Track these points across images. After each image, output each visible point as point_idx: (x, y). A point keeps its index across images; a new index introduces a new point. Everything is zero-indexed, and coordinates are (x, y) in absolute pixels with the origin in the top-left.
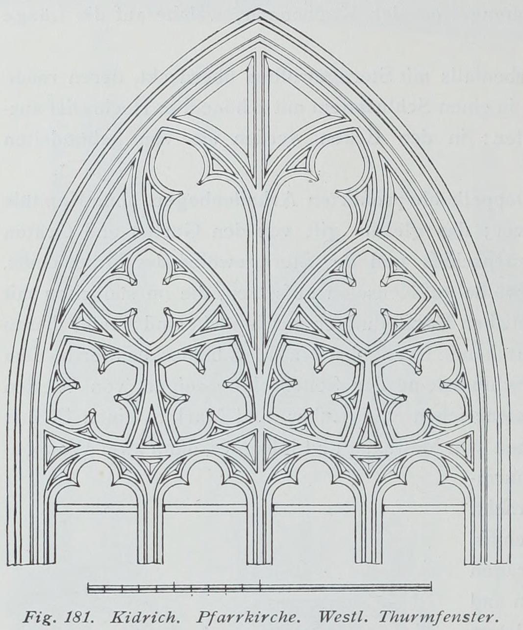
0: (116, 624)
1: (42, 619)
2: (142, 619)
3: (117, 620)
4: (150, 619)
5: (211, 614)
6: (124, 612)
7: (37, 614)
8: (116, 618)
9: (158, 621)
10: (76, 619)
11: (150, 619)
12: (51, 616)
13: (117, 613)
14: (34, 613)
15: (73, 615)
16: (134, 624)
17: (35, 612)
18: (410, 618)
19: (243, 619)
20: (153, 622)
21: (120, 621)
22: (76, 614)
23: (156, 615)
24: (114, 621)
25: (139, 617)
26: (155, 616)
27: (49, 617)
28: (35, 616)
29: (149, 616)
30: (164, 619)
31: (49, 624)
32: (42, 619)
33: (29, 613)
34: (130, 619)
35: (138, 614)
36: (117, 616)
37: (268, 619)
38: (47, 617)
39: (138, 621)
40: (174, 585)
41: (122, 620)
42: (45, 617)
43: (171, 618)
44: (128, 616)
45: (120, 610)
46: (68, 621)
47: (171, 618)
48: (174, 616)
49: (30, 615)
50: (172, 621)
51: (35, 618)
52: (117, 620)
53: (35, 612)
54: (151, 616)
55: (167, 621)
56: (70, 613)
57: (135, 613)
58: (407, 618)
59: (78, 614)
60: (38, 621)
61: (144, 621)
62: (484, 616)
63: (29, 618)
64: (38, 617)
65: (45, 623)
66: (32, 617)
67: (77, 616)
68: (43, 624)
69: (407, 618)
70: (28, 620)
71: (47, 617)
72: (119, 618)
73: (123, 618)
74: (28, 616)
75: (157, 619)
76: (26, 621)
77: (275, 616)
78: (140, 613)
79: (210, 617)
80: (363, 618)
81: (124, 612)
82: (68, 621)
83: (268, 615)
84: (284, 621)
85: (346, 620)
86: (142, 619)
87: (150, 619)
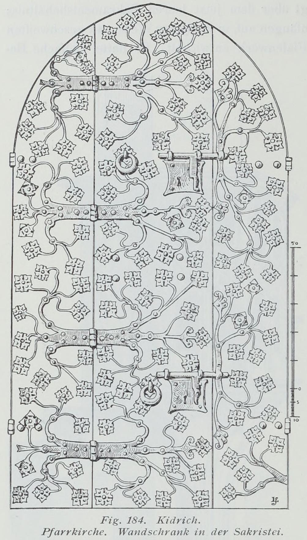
0: (160, 525)
1: (112, 521)
2: (176, 521)
3: (160, 522)
6: (165, 517)
7: (110, 518)
9: (186, 522)
10: (134, 521)
12: (118, 520)
13: (160, 517)
15: (132, 519)
17: (108, 517)
20: (183, 523)
21: (162, 523)
22: (134, 519)
23: (185, 519)
24: (158, 523)
25: (174, 520)
26: (184, 520)
28: (108, 519)
31: (117, 524)
32: (112, 521)
33: (104, 517)
34: (169, 522)
35: (174, 518)
36: (161, 519)
38: (116, 520)
41: (163, 522)
42: (114, 520)
45: (163, 516)
48: (196, 520)
49: (105, 519)
50: (195, 523)
51: (108, 521)
52: (160, 522)
53: (108, 517)
54: (182, 519)
56: (130, 518)
57: (172, 518)
59: (135, 518)
60: (110, 523)
61: (178, 523)
63: (104, 521)
64: (111, 520)
65: (115, 524)
66: (106, 520)
67: (134, 520)
68: (113, 524)
70: (104, 522)
71: (116, 520)
72: (161, 520)
73: (164, 521)
74: (103, 520)
75: (185, 521)
76: (102, 523)
78: (175, 517)
81: (165, 517)
82: (129, 523)
86: (176, 521)
87: (181, 522)
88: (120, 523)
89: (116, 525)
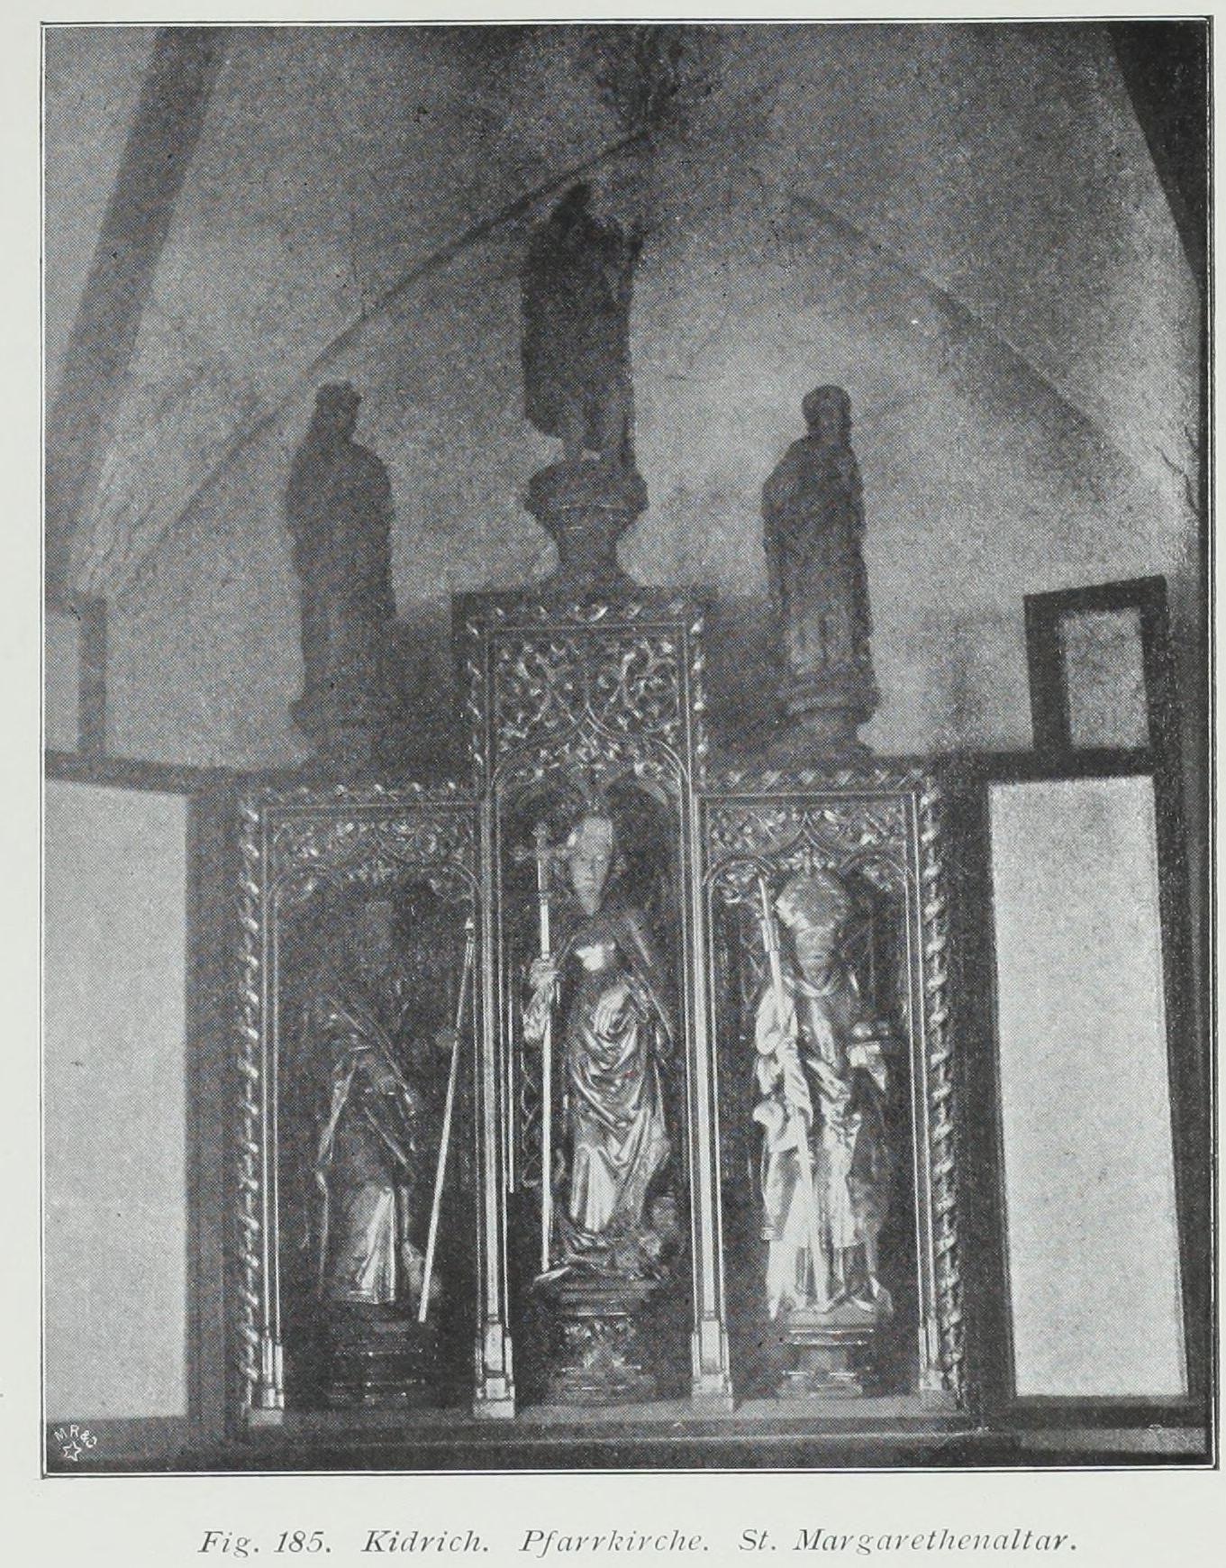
1: (232, 1546)
2: (419, 1543)
3: (373, 1546)
4: (435, 1544)
5: (546, 1536)
8: (372, 1543)
10: (296, 1546)
11: (433, 1545)
15: (290, 1539)
19: (603, 1545)
20: (439, 1549)
21: (379, 1549)
22: (295, 1538)
24: (367, 1549)
32: (232, 1546)
33: (210, 1534)
34: (398, 1544)
37: (650, 1545)
43: (473, 1542)
45: (380, 1528)
47: (473, 1542)
49: (212, 1538)
52: (373, 1546)
56: (285, 1536)
57: (406, 1534)
59: (300, 1537)
63: (210, 1544)
73: (385, 1543)
74: (208, 1541)
75: (446, 1546)
76: (204, 1549)
79: (545, 1540)
86: (419, 1543)
87: (433, 1545)
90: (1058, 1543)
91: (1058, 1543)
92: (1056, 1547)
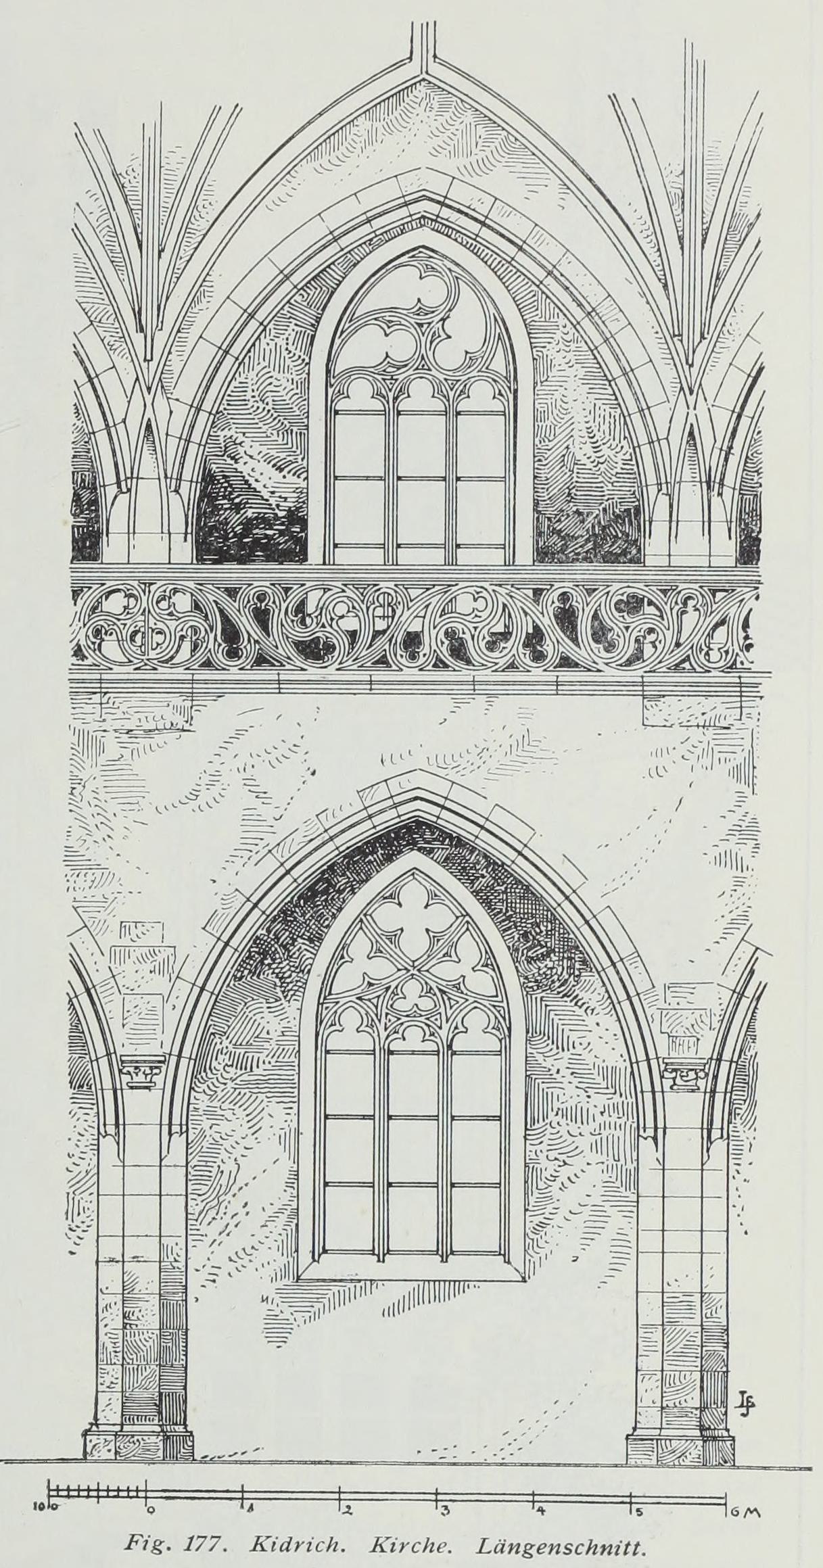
0: (258, 1554)
1: (150, 1546)
3: (259, 1548)
4: (305, 1546)
7: (146, 1538)
8: (258, 1545)
9: (315, 1549)
11: (304, 1547)
13: (259, 1537)
14: (140, 1537)
16: (282, 1553)
17: (142, 1536)
18: (507, 1549)
20: (308, 1550)
25: (289, 1543)
26: (310, 1543)
27: (161, 1543)
28: (141, 1541)
29: (303, 1543)
30: (323, 1547)
32: (150, 1546)
33: (133, 1536)
34: (277, 1547)
35: (288, 1540)
38: (157, 1543)
39: (287, 1550)
40: (243, 1492)
42: (155, 1542)
43: (332, 1546)
44: (274, 1543)
46: (188, 1549)
47: (332, 1546)
48: (337, 1543)
49: (135, 1539)
50: (334, 1550)
51: (141, 1544)
52: (259, 1548)
53: (142, 1536)
55: (328, 1550)
58: (511, 1550)
60: (144, 1549)
62: (546, 1545)
63: (133, 1544)
64: (147, 1541)
66: (137, 1542)
69: (511, 1550)
71: (157, 1543)
73: (267, 1545)
74: (131, 1541)
75: (313, 1547)
76: (129, 1548)
77: (417, 1544)
78: (291, 1538)
80: (339, 1547)
81: (268, 1537)
83: (408, 1543)
84: (431, 1551)
85: (567, 1552)
86: (293, 1546)
87: (304, 1547)
88: (169, 1549)
89: (158, 1552)
90: (403, 1547)
91: (403, 1547)
92: (401, 1551)
